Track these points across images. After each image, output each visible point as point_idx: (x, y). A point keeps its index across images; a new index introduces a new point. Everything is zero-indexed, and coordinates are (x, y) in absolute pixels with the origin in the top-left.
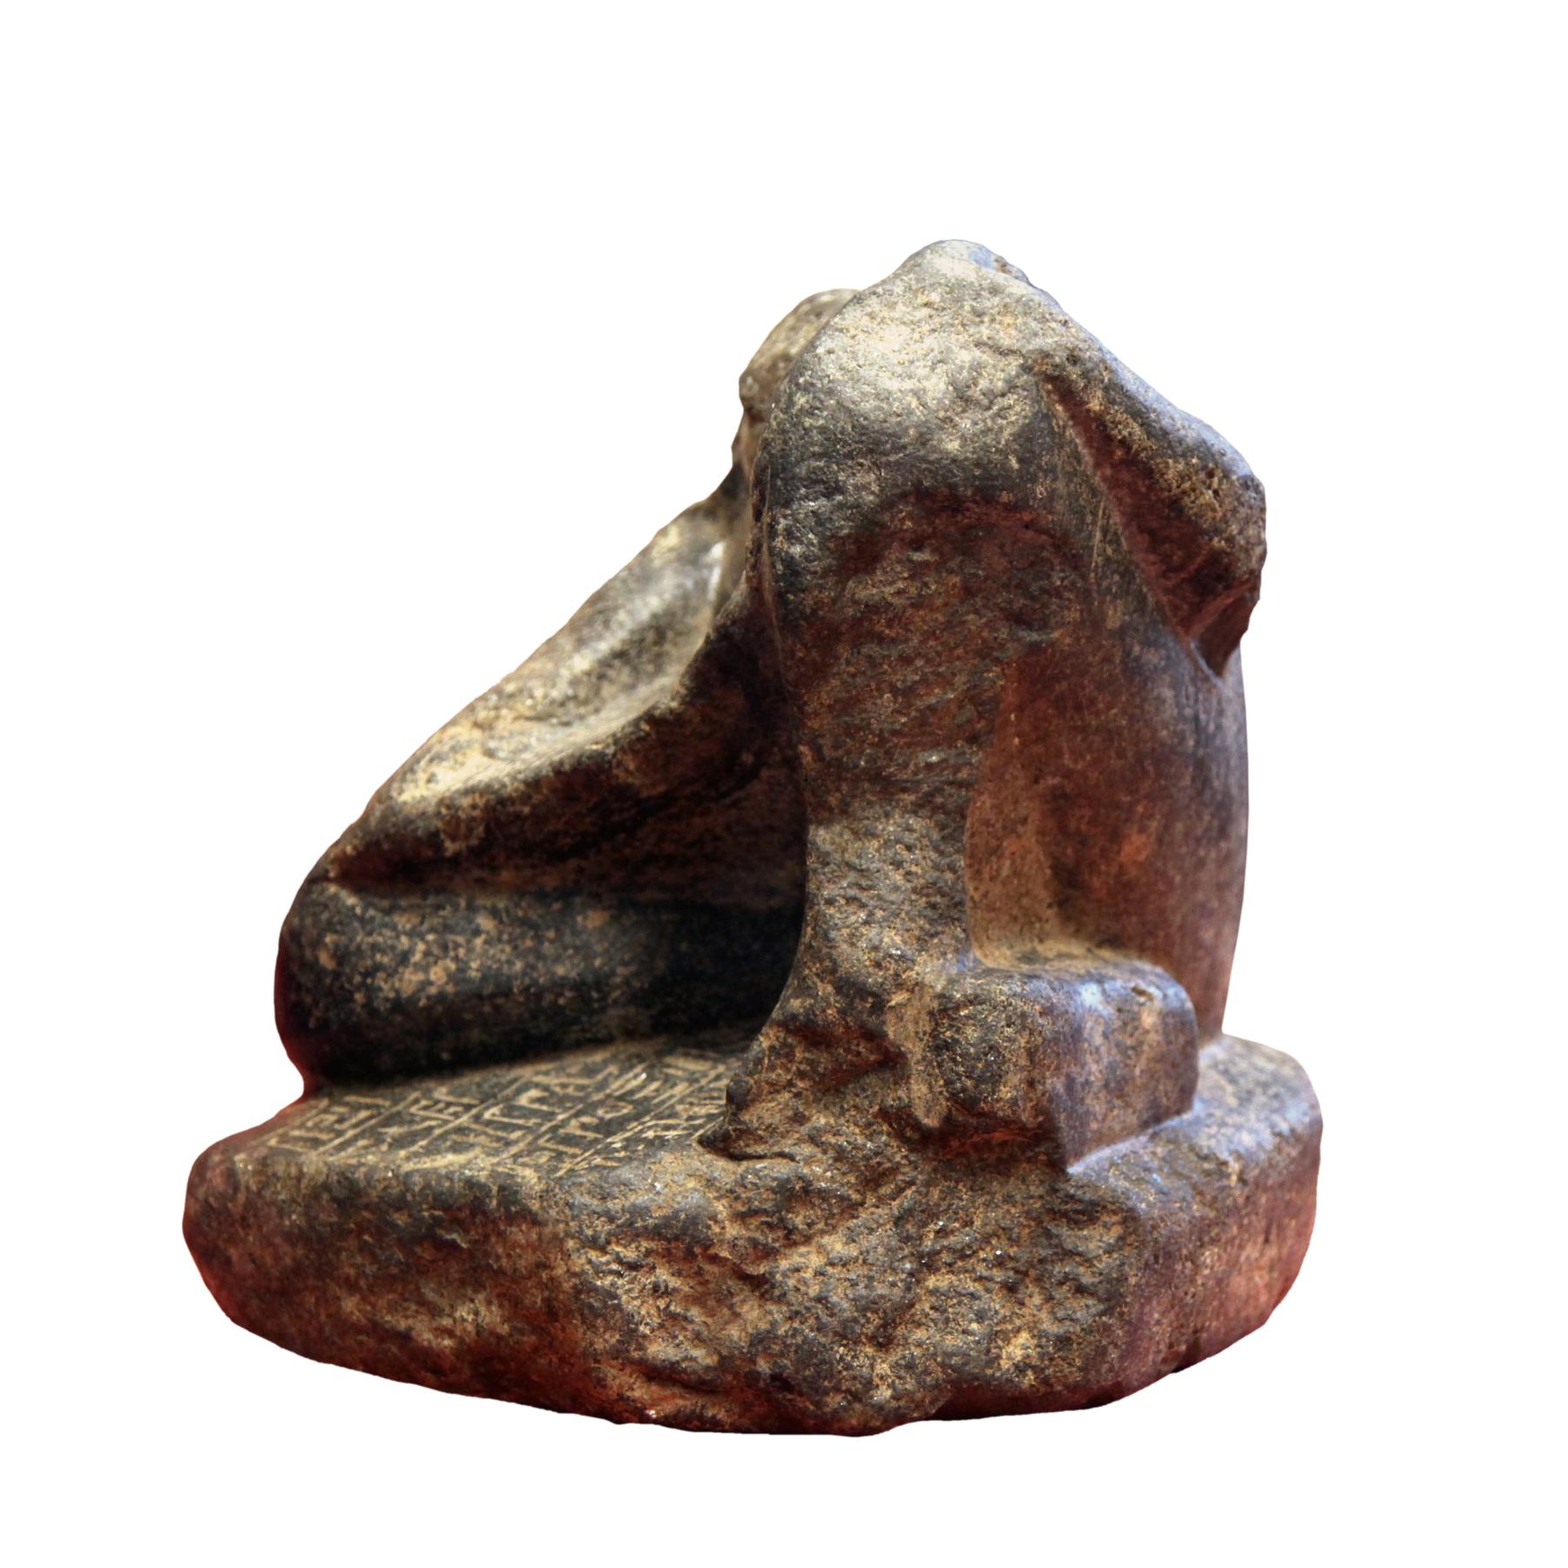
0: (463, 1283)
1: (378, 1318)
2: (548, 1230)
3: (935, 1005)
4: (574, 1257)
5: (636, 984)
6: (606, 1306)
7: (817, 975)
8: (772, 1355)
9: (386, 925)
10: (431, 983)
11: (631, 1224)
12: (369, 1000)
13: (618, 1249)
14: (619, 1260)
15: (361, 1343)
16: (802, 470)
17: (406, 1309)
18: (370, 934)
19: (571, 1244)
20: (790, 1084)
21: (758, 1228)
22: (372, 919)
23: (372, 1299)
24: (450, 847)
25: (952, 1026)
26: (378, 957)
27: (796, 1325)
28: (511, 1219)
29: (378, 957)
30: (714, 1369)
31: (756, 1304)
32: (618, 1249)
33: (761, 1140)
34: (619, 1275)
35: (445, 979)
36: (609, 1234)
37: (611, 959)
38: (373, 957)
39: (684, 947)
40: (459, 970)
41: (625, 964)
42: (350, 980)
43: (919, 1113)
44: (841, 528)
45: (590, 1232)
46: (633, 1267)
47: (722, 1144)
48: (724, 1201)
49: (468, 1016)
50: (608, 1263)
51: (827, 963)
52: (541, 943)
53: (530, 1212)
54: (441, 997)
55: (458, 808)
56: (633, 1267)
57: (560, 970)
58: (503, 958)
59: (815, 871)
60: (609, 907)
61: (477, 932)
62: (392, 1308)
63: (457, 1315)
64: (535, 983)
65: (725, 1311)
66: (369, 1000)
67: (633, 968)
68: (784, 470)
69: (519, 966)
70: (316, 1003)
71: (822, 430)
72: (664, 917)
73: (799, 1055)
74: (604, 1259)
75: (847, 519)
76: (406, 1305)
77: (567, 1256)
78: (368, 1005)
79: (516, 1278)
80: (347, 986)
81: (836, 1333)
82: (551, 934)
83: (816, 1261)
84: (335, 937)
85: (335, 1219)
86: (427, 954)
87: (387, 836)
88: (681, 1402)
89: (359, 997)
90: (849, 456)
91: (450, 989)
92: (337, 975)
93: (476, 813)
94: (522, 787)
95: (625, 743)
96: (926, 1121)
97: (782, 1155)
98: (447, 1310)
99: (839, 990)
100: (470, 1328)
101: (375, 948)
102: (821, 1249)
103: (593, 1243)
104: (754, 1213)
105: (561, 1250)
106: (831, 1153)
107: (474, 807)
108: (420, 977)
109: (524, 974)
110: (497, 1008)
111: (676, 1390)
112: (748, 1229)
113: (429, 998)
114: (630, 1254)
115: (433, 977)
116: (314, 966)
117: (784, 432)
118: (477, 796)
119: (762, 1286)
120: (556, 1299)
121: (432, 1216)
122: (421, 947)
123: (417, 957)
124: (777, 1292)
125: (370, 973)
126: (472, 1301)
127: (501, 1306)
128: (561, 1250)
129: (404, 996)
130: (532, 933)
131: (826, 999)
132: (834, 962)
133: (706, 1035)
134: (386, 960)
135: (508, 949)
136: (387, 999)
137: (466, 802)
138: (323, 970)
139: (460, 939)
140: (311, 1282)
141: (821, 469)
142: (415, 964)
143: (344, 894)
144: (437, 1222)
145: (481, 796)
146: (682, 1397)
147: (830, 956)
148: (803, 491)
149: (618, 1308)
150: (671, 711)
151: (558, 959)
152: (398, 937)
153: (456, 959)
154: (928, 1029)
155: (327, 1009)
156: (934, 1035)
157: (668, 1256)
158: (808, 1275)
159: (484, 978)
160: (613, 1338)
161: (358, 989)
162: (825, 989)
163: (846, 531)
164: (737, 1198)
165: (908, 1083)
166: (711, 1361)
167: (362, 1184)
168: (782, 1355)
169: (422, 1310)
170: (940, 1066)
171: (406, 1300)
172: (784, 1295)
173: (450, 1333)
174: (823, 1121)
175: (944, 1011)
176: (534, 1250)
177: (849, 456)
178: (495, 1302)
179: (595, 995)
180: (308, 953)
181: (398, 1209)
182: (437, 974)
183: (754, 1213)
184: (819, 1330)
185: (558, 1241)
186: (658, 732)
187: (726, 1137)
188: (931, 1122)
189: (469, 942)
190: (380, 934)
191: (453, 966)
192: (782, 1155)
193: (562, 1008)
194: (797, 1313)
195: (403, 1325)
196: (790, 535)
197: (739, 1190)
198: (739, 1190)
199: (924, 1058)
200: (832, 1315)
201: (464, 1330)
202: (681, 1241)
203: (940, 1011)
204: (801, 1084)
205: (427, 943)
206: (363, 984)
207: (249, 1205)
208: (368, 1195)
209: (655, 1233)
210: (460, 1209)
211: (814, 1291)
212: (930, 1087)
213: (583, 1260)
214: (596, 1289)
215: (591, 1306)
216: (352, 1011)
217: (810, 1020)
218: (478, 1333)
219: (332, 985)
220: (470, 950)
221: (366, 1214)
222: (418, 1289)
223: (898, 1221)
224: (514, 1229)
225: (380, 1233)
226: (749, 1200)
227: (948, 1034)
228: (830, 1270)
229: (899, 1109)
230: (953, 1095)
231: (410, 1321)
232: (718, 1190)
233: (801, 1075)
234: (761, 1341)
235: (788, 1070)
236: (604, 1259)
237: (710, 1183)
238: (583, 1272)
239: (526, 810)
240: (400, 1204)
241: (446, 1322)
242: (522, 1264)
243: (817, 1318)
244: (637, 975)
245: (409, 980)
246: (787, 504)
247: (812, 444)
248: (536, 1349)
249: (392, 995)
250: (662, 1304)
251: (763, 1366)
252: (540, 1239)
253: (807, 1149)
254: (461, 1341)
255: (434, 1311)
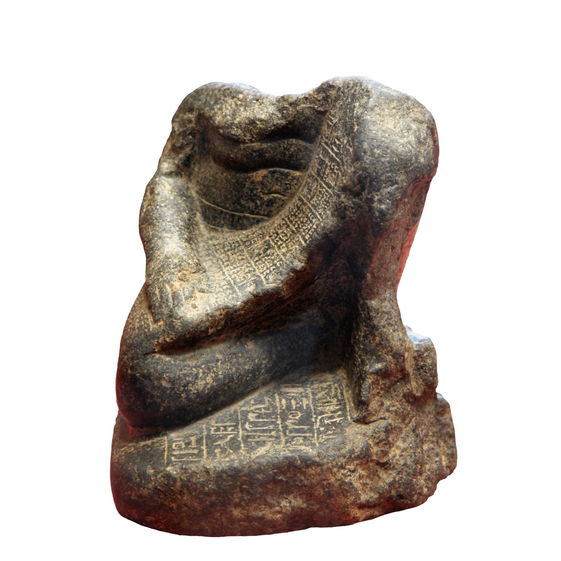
0: (281, 493)
1: (250, 514)
2: (325, 467)
3: (416, 354)
4: (337, 474)
5: (269, 366)
6: (350, 488)
7: (386, 354)
8: (396, 488)
9: (185, 366)
10: (208, 384)
11: (350, 457)
12: (188, 395)
13: (348, 467)
14: (350, 471)
15: (241, 526)
16: (383, 178)
17: (260, 508)
18: (181, 370)
19: (335, 470)
20: (379, 393)
21: (382, 446)
22: (179, 364)
23: (247, 508)
24: (210, 331)
25: (422, 360)
26: (187, 378)
27: (400, 476)
28: (308, 466)
29: (187, 378)
30: (378, 498)
31: (384, 472)
32: (348, 467)
33: (374, 415)
34: (350, 475)
35: (212, 381)
36: (346, 462)
37: (260, 359)
38: (185, 379)
39: (279, 348)
40: (216, 376)
41: (264, 359)
42: (178, 390)
43: (415, 392)
44: (398, 197)
45: (340, 464)
46: (353, 472)
47: (363, 421)
48: (370, 440)
49: (220, 393)
50: (347, 473)
51: (389, 349)
52: (238, 359)
53: (316, 462)
54: (212, 387)
55: (215, 316)
56: (353, 472)
57: (247, 367)
58: (228, 368)
59: (375, 317)
60: (252, 339)
61: (218, 360)
62: (255, 509)
63: (282, 505)
64: (240, 374)
65: (376, 477)
66: (188, 395)
67: (267, 360)
68: (376, 178)
69: (234, 370)
70: (163, 401)
71: (389, 162)
72: (269, 339)
73: (381, 383)
74: (345, 472)
75: (400, 193)
76: (260, 507)
77: (334, 474)
78: (188, 398)
79: (312, 486)
80: (178, 392)
81: (413, 475)
82: (240, 355)
83: (398, 452)
84: (168, 374)
85: (231, 483)
86: (204, 373)
87: (189, 332)
88: (367, 513)
89: (183, 395)
90: (398, 170)
91: (215, 384)
92: (172, 389)
93: (221, 317)
94: (243, 304)
95: (285, 282)
96: (417, 394)
97: (381, 419)
98: (276, 504)
99: (394, 357)
100: (289, 508)
101: (185, 375)
102: (398, 447)
103: (342, 467)
104: (381, 441)
105: (332, 473)
106: (394, 414)
107: (221, 315)
108: (204, 382)
109: (236, 372)
110: (229, 387)
111: (367, 509)
112: (380, 447)
113: (208, 389)
114: (352, 467)
115: (208, 381)
116: (160, 387)
117: (374, 164)
118: (222, 310)
119: (385, 466)
120: (332, 490)
121: (274, 473)
122: (201, 371)
123: (201, 375)
124: (392, 466)
125: (186, 386)
126: (287, 498)
127: (302, 498)
128: (332, 473)
129: (200, 391)
130: (234, 356)
131: (390, 361)
132: (392, 348)
133: (286, 378)
134: (190, 379)
135: (229, 364)
136: (194, 394)
137: (217, 313)
138: (165, 388)
139: (213, 365)
140: (218, 508)
141: (390, 176)
142: (201, 378)
143: (163, 357)
144: (276, 474)
145: (223, 310)
146: (368, 511)
147: (389, 346)
148: (384, 185)
149: (353, 487)
150: (303, 267)
151: (245, 364)
152: (191, 369)
153: (214, 372)
154: (414, 363)
155: (169, 403)
156: (417, 365)
157: (361, 464)
158: (398, 457)
159: (224, 377)
160: (352, 498)
161: (183, 392)
162: (389, 358)
163: (399, 197)
164: (375, 438)
165: (410, 383)
166: (376, 496)
167: (240, 468)
168: (399, 487)
169: (267, 507)
170: (420, 374)
171: (260, 505)
172: (394, 467)
173: (279, 512)
174: (388, 403)
175: (419, 356)
176: (319, 475)
177: (398, 170)
178: (298, 496)
179: (257, 373)
180: (156, 383)
181: (259, 473)
182: (209, 380)
183: (381, 441)
184: (408, 475)
185: (330, 470)
186: (296, 275)
187: (365, 417)
188: (418, 394)
189: (216, 365)
190: (185, 369)
191: (213, 375)
192: (381, 419)
193: (248, 381)
194: (400, 472)
195: (260, 514)
196: (380, 201)
197: (374, 435)
198: (374, 435)
199: (414, 373)
200: (410, 469)
201: (287, 510)
202: (364, 458)
203: (418, 356)
204: (382, 392)
205: (202, 369)
206: (184, 390)
207: (182, 486)
208: (243, 471)
209: (358, 458)
210: (283, 467)
211: (402, 462)
212: (417, 383)
213: (340, 475)
214: (346, 483)
215: (345, 489)
216: (181, 401)
217: (387, 370)
218: (293, 510)
219: (170, 394)
220: (217, 368)
221: (244, 478)
222: (265, 500)
223: (414, 431)
224: (310, 469)
225: (251, 484)
226: (379, 437)
227: (422, 363)
228: (403, 454)
229: (410, 392)
230: (426, 384)
231: (263, 512)
232: (368, 436)
233: (382, 389)
234: (391, 485)
235: (378, 389)
236: (345, 472)
237: (364, 435)
238: (342, 478)
239: (243, 312)
240: (259, 471)
241: (277, 508)
242: (314, 481)
243: (406, 471)
244: (268, 362)
245: (200, 384)
246: (378, 190)
247: (387, 168)
248: (318, 509)
249: (196, 392)
250: (361, 481)
251: (393, 493)
252: (322, 471)
253: (387, 414)
254: (285, 513)
255: (271, 506)
